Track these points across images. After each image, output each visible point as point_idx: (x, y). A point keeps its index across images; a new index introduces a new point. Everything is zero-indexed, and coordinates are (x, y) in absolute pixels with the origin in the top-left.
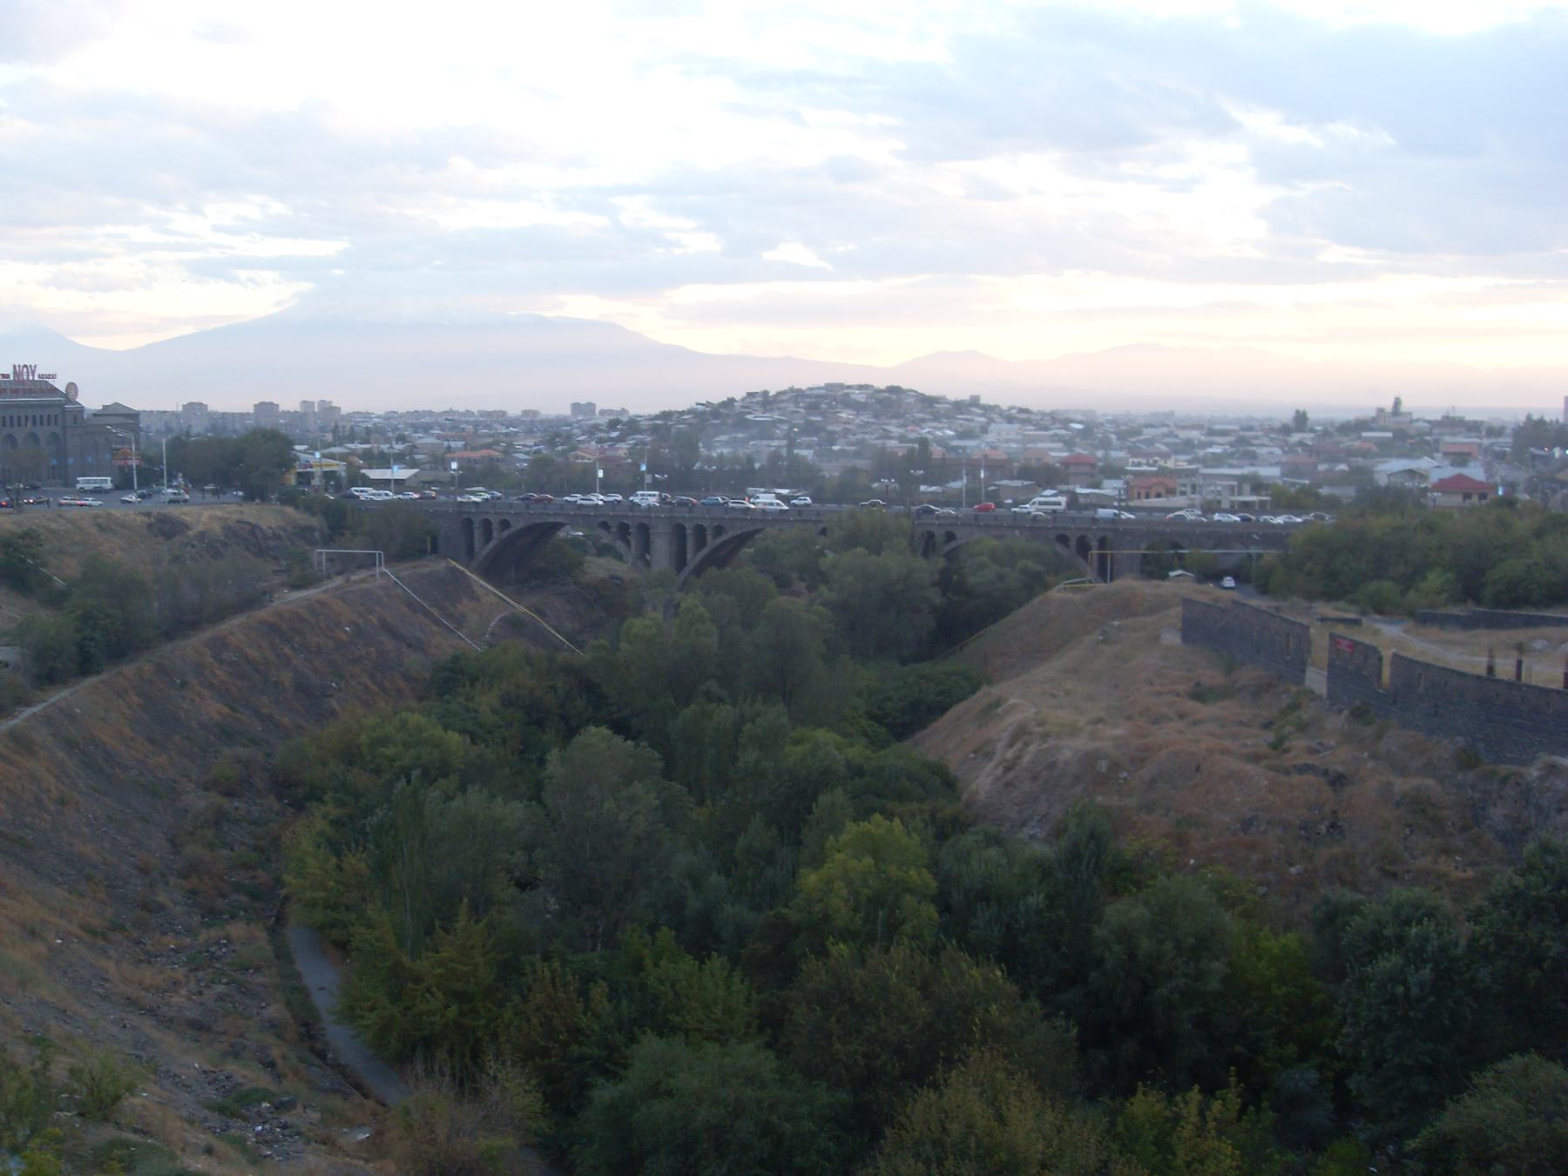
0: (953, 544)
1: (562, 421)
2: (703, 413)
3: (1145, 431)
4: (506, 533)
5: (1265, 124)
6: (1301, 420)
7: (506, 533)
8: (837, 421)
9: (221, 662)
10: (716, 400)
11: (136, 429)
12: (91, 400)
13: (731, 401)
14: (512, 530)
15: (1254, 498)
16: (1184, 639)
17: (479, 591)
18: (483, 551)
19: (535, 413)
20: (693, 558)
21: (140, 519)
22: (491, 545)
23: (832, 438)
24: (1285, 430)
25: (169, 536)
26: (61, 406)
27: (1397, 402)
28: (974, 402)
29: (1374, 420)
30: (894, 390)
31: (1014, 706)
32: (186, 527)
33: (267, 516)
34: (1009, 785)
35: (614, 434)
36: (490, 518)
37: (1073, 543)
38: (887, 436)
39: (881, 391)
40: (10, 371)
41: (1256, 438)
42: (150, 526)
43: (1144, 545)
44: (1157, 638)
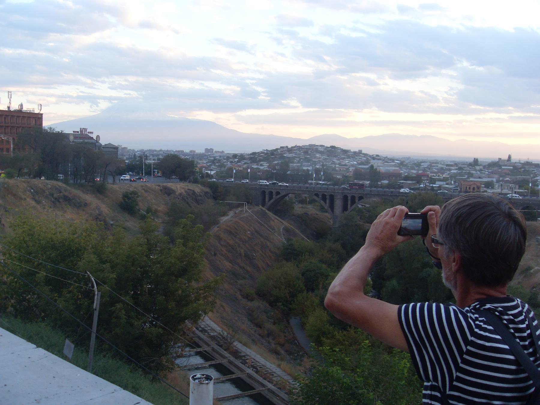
1: (203, 154)
2: (266, 154)
3: (422, 164)
4: (278, 196)
6: (476, 162)
7: (278, 196)
8: (316, 158)
9: (222, 245)
10: (270, 149)
11: (116, 153)
12: (103, 142)
13: (277, 149)
18: (268, 203)
19: (194, 151)
21: (157, 187)
22: (272, 201)
23: (315, 163)
24: (470, 165)
25: (169, 194)
27: (510, 157)
28: (360, 152)
29: (498, 162)
33: (197, 188)
36: (272, 190)
38: (334, 163)
39: (328, 147)
40: (79, 130)
41: (465, 167)
42: (161, 190)
43: (521, 208)
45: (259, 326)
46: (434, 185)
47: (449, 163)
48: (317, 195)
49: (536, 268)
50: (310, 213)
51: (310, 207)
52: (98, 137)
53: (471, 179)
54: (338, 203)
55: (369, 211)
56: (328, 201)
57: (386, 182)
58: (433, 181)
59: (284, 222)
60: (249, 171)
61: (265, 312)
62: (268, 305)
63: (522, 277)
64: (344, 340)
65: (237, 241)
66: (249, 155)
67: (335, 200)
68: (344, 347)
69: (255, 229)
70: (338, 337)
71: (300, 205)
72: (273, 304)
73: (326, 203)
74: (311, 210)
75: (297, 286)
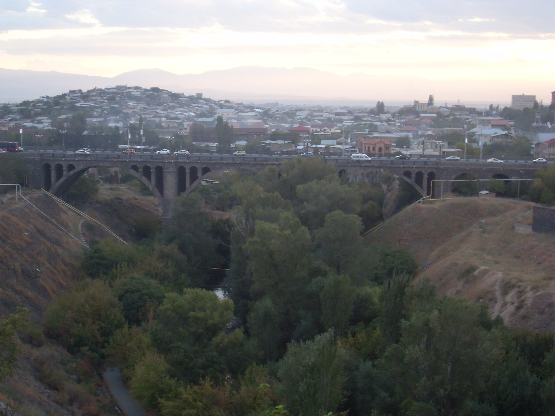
2: (47, 103)
3: (298, 113)
4: (72, 172)
6: (381, 108)
7: (72, 172)
8: (128, 107)
13: (64, 95)
14: (75, 171)
16: (534, 229)
17: (64, 207)
18: (56, 184)
22: (62, 180)
23: (127, 116)
24: (372, 112)
27: (431, 99)
28: (199, 96)
30: (156, 90)
31: (485, 272)
34: (524, 317)
36: (62, 163)
37: (413, 176)
38: (157, 115)
39: (148, 90)
41: (364, 117)
43: (454, 177)
44: (513, 228)
45: (54, 387)
46: (319, 146)
47: (339, 111)
48: (135, 168)
49: (483, 268)
50: (124, 197)
51: (123, 187)
53: (376, 135)
54: (170, 181)
55: (219, 191)
56: (153, 177)
57: (243, 143)
58: (317, 139)
59: (82, 213)
60: (21, 131)
61: (62, 363)
62: (65, 352)
63: (462, 282)
64: (195, 400)
65: (7, 248)
66: (17, 106)
67: (165, 174)
68: (195, 411)
69: (36, 227)
70: (185, 396)
71: (108, 186)
72: (73, 349)
73: (149, 179)
74: (127, 192)
75: (112, 316)
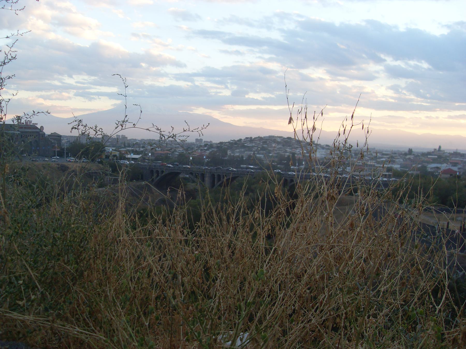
0: (293, 183)
1: (192, 144)
2: (232, 143)
5: (390, 61)
6: (410, 151)
7: (163, 175)
10: (236, 140)
12: (48, 131)
13: (241, 140)
15: (387, 173)
20: (217, 184)
22: (159, 177)
24: (406, 154)
26: (38, 132)
27: (440, 147)
29: (433, 152)
32: (68, 168)
33: (93, 167)
35: (206, 148)
36: (159, 170)
38: (286, 152)
39: (285, 138)
41: (396, 156)
42: (58, 168)
47: (384, 152)
52: (42, 127)
